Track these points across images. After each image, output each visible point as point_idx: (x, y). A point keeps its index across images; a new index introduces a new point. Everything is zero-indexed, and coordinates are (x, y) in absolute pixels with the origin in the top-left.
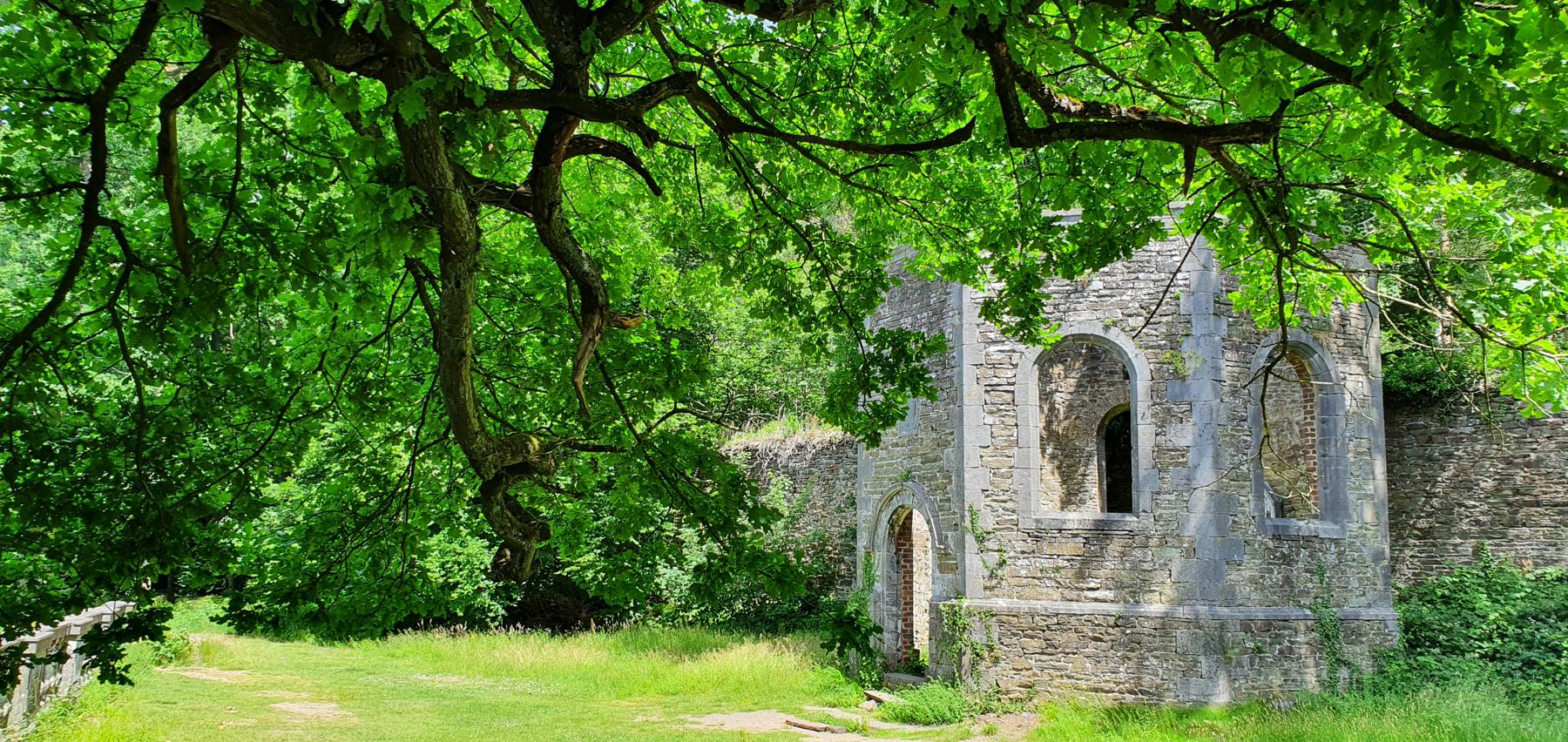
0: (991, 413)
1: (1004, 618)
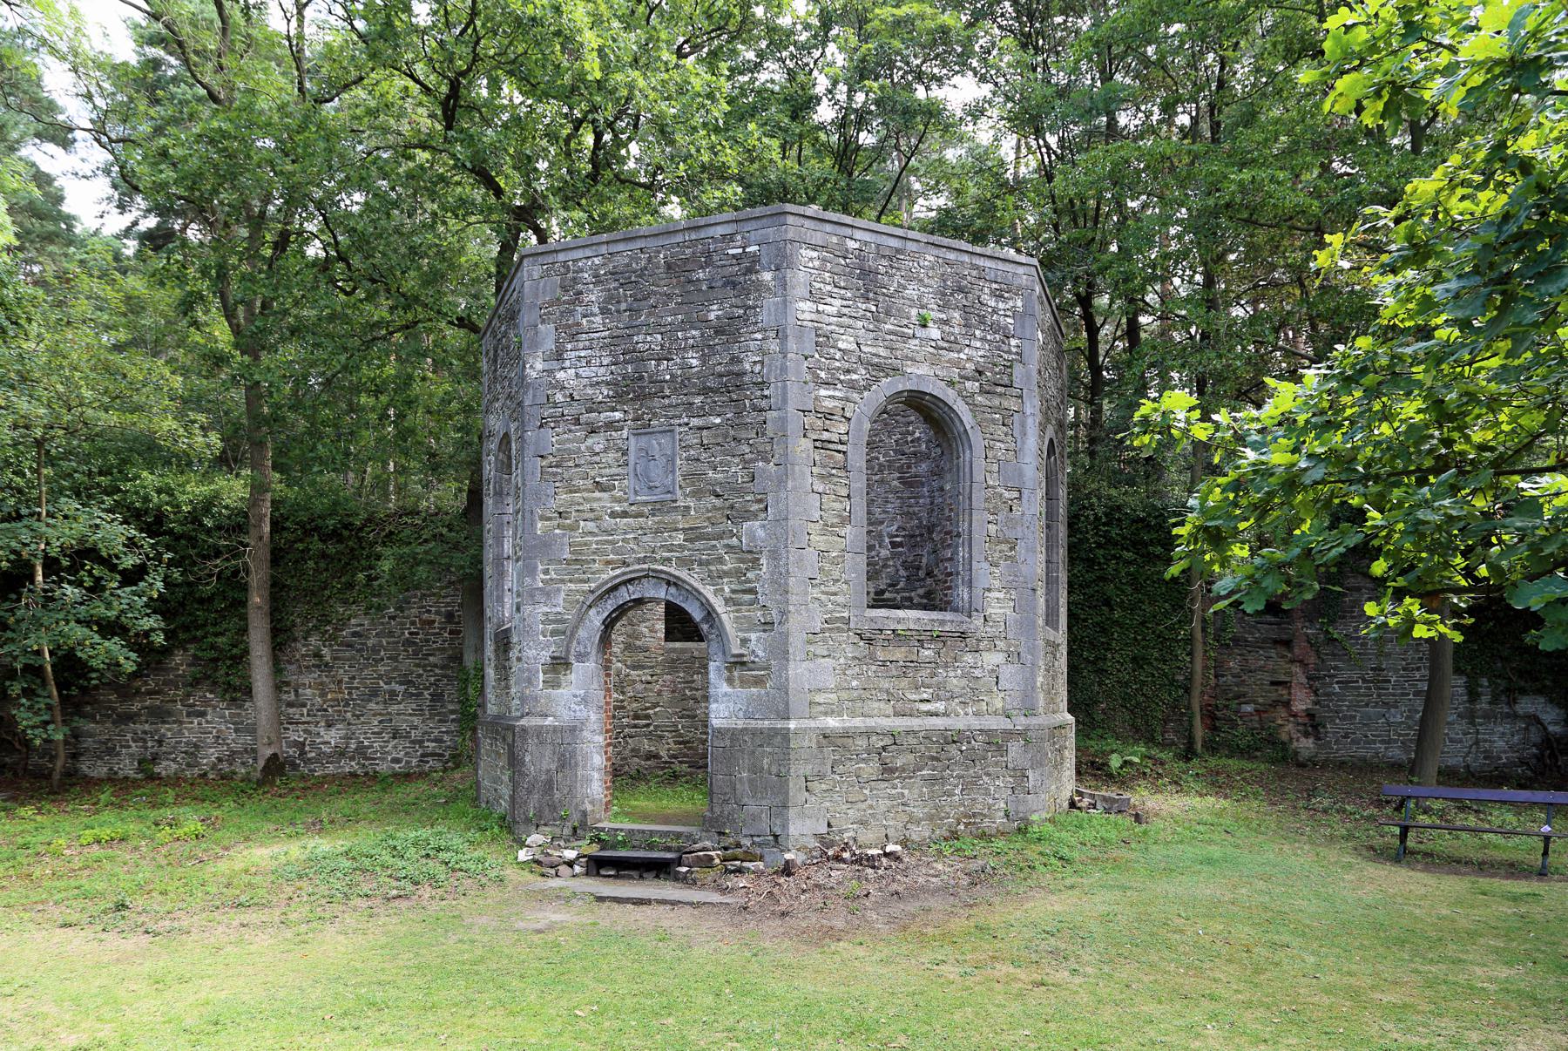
0: (821, 477)
1: (839, 742)
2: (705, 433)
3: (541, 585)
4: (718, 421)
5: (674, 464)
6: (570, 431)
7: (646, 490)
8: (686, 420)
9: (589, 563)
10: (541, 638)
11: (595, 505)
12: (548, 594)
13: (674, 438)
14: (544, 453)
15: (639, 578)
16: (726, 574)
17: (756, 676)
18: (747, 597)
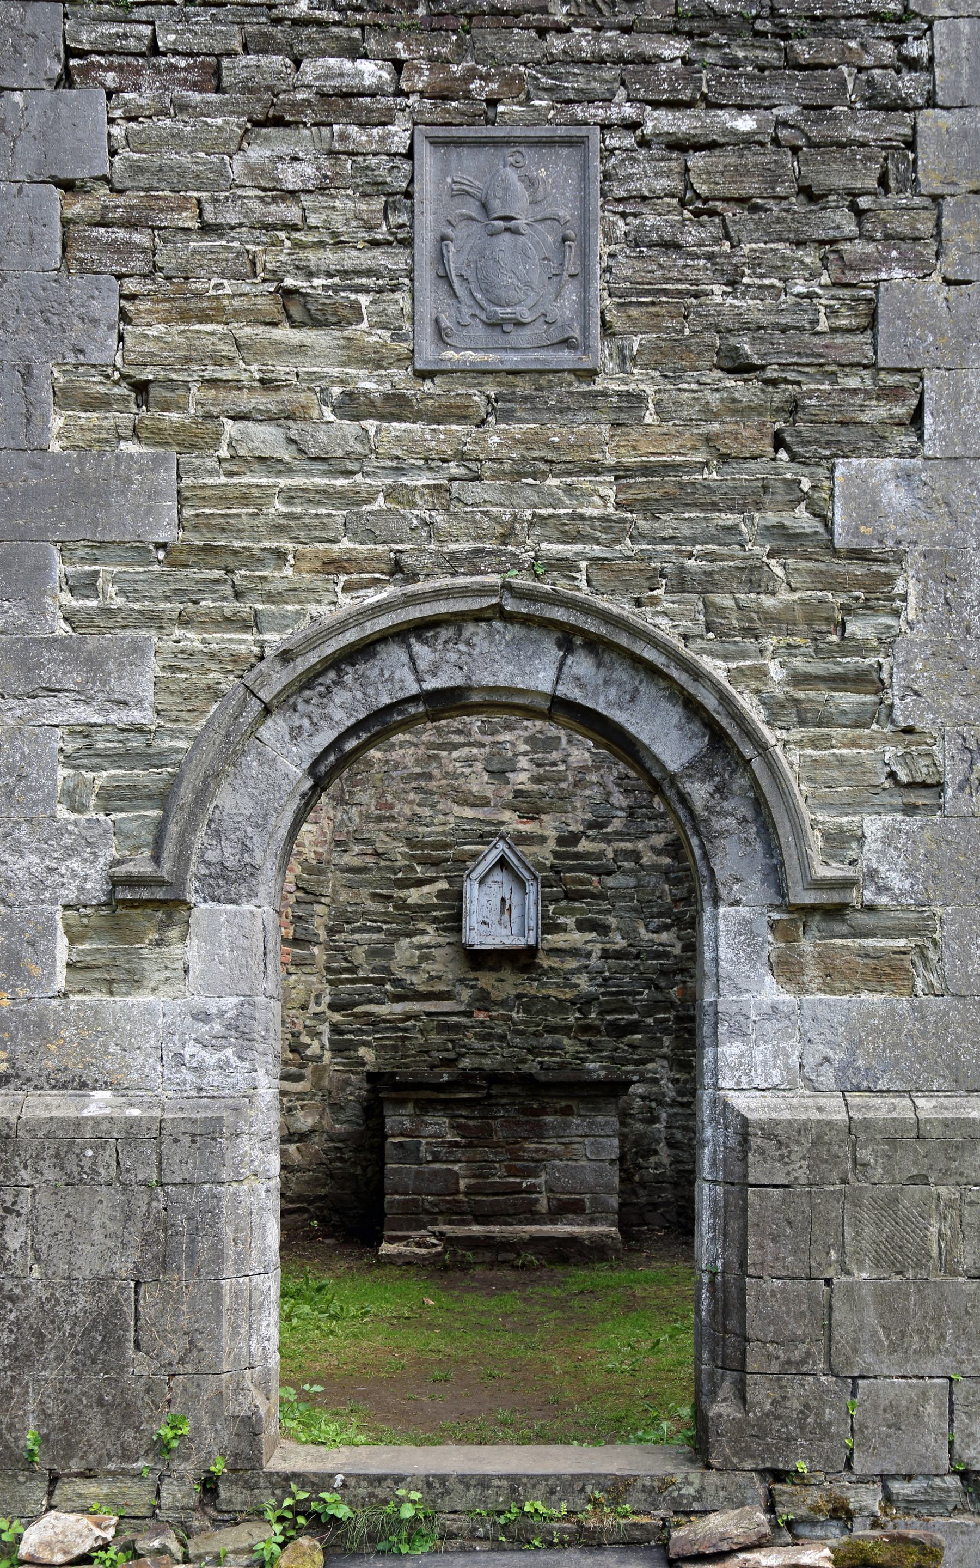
2: (696, 160)
3: (62, 629)
4: (745, 123)
5: (585, 255)
6: (182, 107)
7: (478, 330)
8: (629, 111)
9: (253, 560)
10: (62, 812)
11: (281, 369)
12: (94, 663)
13: (585, 167)
14: (80, 173)
15: (457, 620)
16: (773, 621)
17: (877, 955)
18: (847, 699)
